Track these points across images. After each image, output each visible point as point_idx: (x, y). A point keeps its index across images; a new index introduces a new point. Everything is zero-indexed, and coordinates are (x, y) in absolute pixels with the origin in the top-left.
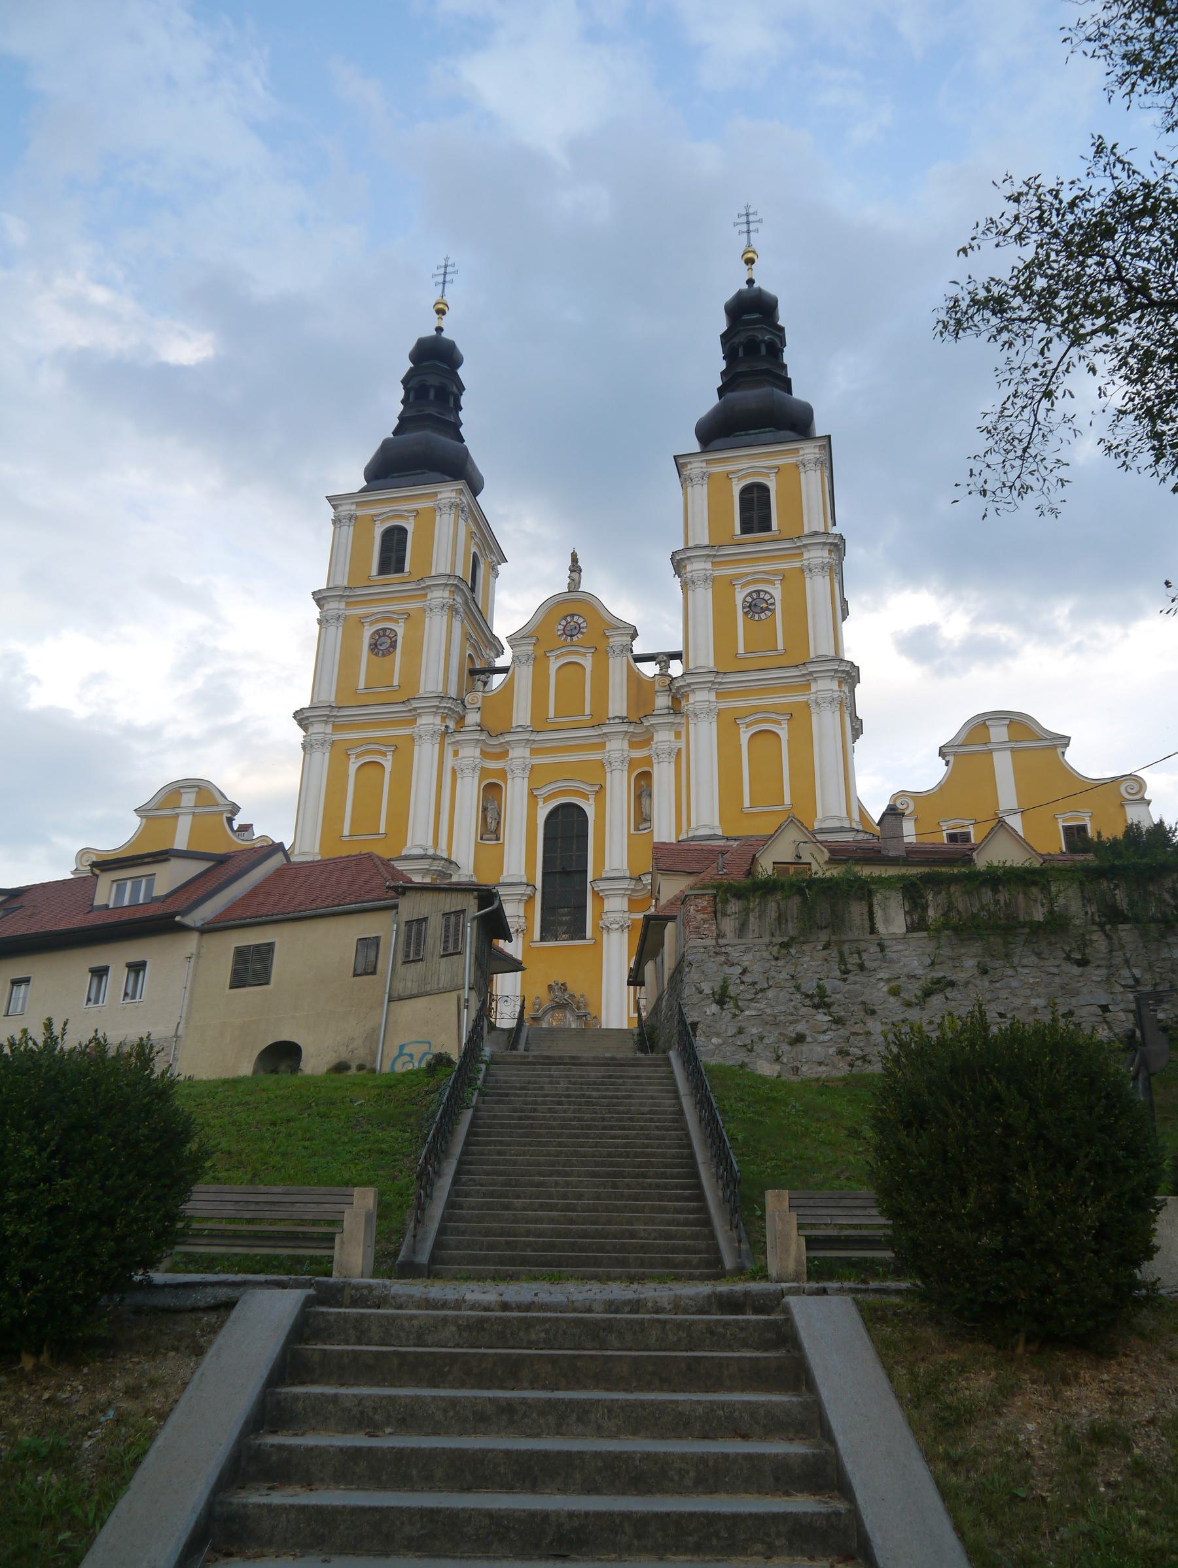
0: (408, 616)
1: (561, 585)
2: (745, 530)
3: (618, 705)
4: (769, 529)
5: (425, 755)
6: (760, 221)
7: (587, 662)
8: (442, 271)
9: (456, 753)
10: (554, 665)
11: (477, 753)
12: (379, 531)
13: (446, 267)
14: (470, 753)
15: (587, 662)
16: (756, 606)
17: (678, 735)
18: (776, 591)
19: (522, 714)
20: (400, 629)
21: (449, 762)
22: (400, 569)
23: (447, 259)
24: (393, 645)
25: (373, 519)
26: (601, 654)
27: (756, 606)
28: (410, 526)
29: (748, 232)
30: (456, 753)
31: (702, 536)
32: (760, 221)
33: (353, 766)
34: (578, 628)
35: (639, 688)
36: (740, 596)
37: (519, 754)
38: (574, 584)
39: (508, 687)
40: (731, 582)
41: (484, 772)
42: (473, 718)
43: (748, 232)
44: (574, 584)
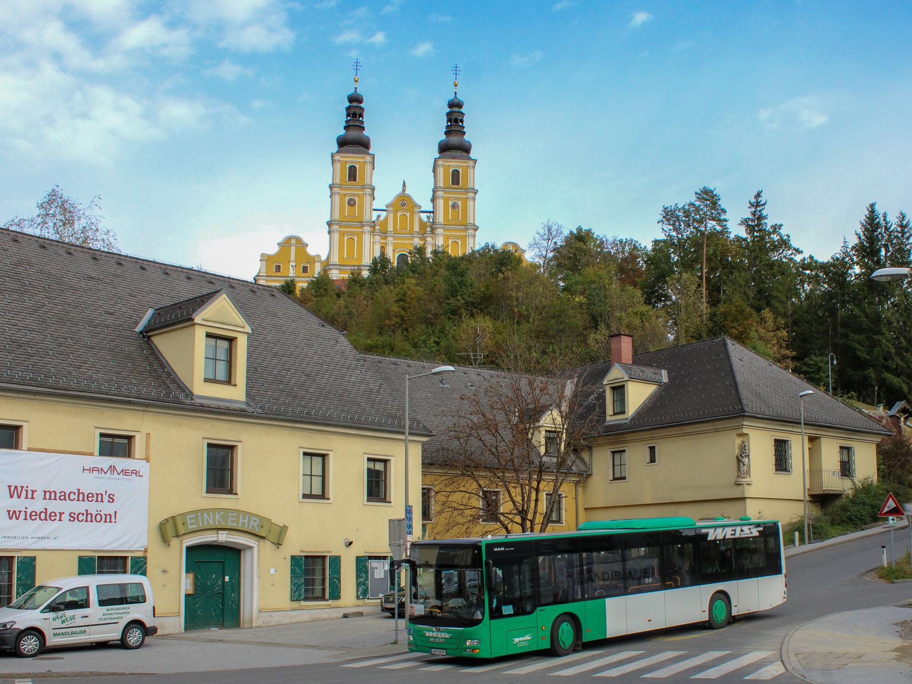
0: (358, 195)
1: (399, 190)
2: (452, 184)
3: (416, 228)
4: (459, 184)
5: (367, 238)
6: (460, 71)
7: (408, 215)
8: (356, 64)
9: (373, 237)
10: (399, 214)
11: (379, 238)
12: (348, 166)
13: (357, 63)
14: (377, 238)
15: (408, 215)
16: (454, 206)
17: (433, 239)
18: (460, 203)
19: (390, 228)
20: (356, 199)
21: (372, 240)
22: (355, 180)
23: (357, 60)
24: (355, 203)
25: (346, 162)
26: (412, 213)
27: (454, 206)
28: (357, 166)
29: (456, 74)
30: (373, 237)
31: (441, 184)
32: (460, 71)
33: (346, 238)
34: (405, 204)
35: (423, 225)
36: (451, 203)
37: (390, 239)
38: (404, 190)
39: (386, 218)
40: (448, 199)
41: (381, 243)
42: (377, 227)
43: (456, 74)
44: (404, 190)
